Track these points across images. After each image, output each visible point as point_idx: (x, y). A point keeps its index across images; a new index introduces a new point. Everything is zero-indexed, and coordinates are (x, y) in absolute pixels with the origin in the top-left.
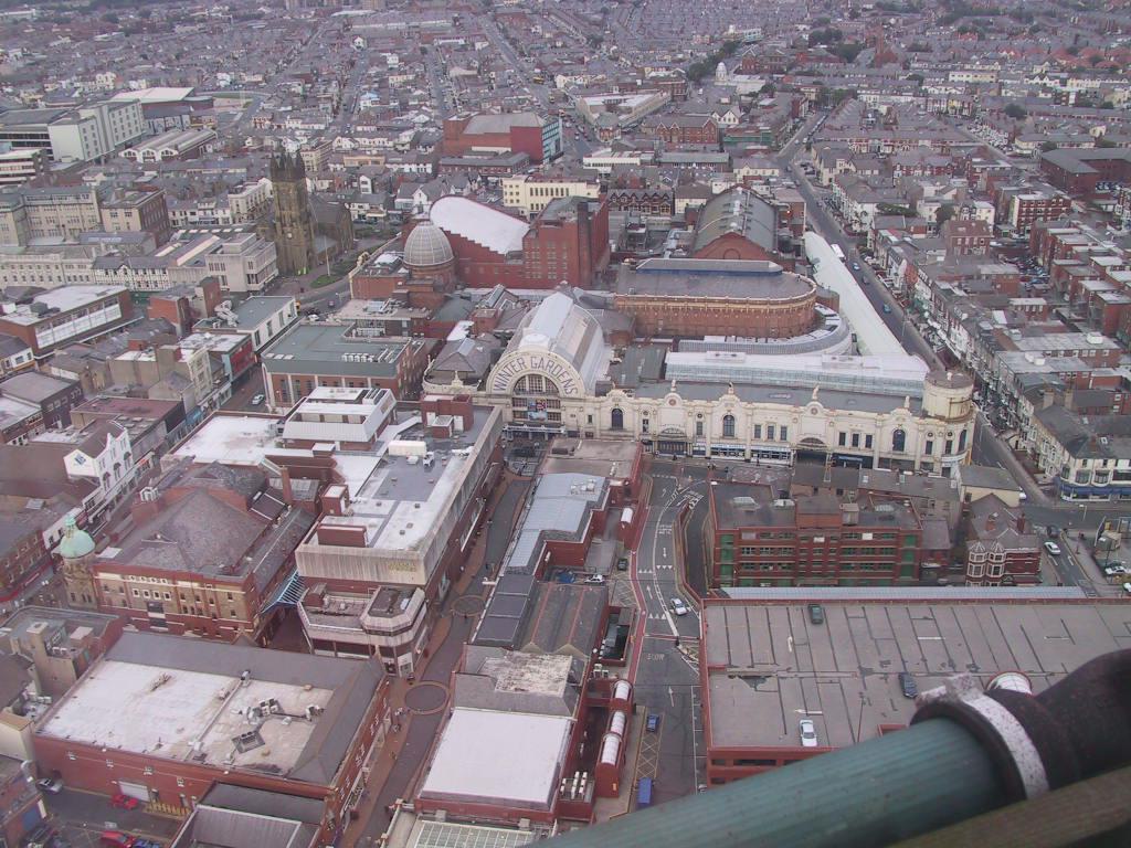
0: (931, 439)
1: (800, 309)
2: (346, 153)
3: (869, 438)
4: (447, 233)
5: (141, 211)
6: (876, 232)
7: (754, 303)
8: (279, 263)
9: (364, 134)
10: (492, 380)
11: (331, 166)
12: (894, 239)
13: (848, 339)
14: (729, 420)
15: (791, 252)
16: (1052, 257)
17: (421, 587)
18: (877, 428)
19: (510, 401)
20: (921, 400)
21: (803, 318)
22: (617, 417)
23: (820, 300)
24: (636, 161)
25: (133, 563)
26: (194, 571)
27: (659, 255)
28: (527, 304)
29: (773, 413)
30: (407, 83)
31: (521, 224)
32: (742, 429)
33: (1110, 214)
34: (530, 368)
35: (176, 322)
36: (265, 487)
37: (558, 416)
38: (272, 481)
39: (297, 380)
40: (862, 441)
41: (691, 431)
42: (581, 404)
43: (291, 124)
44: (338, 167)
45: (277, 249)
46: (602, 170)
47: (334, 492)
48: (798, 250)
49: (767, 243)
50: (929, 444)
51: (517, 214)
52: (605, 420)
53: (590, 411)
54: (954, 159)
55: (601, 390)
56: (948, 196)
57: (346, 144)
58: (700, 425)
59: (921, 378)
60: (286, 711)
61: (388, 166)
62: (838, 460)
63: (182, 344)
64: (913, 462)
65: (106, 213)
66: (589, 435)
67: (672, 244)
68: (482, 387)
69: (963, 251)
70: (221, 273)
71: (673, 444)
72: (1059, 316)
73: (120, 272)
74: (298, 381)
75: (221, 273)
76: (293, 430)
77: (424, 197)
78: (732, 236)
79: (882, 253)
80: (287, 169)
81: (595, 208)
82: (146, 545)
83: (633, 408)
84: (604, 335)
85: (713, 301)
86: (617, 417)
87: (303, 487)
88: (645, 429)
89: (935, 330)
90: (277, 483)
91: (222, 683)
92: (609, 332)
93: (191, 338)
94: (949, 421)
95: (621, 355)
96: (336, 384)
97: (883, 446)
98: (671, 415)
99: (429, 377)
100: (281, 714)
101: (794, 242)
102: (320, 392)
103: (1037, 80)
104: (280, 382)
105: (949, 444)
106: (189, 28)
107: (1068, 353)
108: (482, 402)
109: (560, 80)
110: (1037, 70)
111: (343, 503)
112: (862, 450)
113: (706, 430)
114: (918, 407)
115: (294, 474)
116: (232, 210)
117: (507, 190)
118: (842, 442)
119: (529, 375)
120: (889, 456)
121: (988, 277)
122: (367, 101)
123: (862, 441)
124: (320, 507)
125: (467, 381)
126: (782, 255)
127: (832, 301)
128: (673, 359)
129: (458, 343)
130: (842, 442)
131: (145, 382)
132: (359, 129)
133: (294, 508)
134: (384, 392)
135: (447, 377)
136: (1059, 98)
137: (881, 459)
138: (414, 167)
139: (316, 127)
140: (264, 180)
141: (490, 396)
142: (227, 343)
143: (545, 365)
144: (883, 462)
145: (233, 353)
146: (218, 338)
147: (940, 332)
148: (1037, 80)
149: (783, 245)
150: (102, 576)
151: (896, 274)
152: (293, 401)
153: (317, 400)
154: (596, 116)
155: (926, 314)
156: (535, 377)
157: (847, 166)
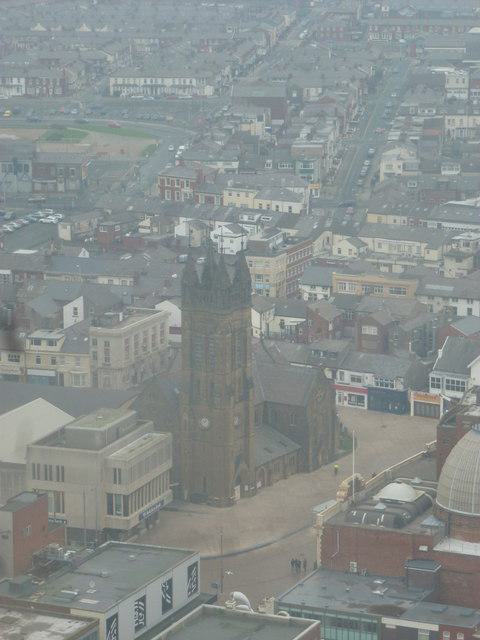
2: (341, 265)
8: (174, 474)
9: (383, 232)
11: (306, 290)
43: (234, 198)
44: (320, 292)
57: (343, 247)
61: (425, 301)
70: (54, 485)
80: (216, 288)
116: (95, 357)
122: (394, 161)
132: (372, 218)
139: (284, 207)
140: (166, 306)
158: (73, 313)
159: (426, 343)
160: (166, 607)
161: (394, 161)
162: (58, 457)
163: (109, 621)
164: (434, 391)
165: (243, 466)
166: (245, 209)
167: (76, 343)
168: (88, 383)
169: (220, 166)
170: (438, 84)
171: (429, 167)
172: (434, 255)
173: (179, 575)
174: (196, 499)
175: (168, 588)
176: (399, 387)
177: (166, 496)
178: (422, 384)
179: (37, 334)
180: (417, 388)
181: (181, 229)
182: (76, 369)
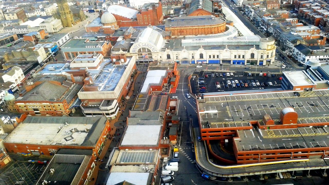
0: (262, 55)
1: (221, 26)
4: (114, 14)
5: (17, 14)
14: (201, 56)
16: (299, 8)
17: (116, 99)
19: (137, 54)
20: (259, 46)
23: (227, 24)
25: (27, 100)
26: (47, 100)
27: (178, 16)
28: (139, 31)
29: (215, 52)
31: (136, 11)
34: (142, 46)
35: (33, 41)
37: (151, 57)
42: (157, 54)
45: (62, 22)
47: (86, 79)
48: (220, 12)
49: (211, 11)
50: (262, 57)
51: (133, 8)
53: (160, 55)
55: (163, 50)
58: (193, 57)
59: (259, 40)
60: (79, 130)
63: (35, 46)
64: (257, 61)
67: (182, 13)
68: (129, 51)
69: (271, 8)
70: (44, 28)
72: (303, 23)
74: (73, 53)
75: (44, 28)
79: (246, 10)
82: (30, 96)
83: (173, 54)
84: (163, 37)
87: (79, 78)
88: (177, 58)
89: (263, 28)
91: (59, 126)
92: (164, 36)
94: (267, 50)
95: (169, 41)
97: (248, 57)
98: (184, 54)
100: (77, 131)
101: (219, 10)
102: (79, 55)
107: (304, 31)
113: (195, 57)
114: (258, 47)
119: (142, 48)
120: (249, 60)
124: (83, 83)
125: (124, 50)
126: (215, 13)
128: (183, 41)
131: (25, 56)
134: (99, 55)
137: (247, 61)
142: (49, 46)
143: (146, 45)
144: (248, 62)
145: (51, 48)
147: (264, 29)
149: (216, 11)
150: (18, 104)
151: (251, 15)
152: (72, 58)
153: (79, 58)
155: (260, 25)
156: (144, 49)
158: (41, 7)
159: (95, 4)
162: (44, 25)
163: (58, 43)
164: (98, 9)
165: (72, 22)
167: (43, 10)
168: (46, 15)
174: (66, 27)
176: (92, 9)
178: (96, 8)
179: (36, 10)
180: (95, 9)
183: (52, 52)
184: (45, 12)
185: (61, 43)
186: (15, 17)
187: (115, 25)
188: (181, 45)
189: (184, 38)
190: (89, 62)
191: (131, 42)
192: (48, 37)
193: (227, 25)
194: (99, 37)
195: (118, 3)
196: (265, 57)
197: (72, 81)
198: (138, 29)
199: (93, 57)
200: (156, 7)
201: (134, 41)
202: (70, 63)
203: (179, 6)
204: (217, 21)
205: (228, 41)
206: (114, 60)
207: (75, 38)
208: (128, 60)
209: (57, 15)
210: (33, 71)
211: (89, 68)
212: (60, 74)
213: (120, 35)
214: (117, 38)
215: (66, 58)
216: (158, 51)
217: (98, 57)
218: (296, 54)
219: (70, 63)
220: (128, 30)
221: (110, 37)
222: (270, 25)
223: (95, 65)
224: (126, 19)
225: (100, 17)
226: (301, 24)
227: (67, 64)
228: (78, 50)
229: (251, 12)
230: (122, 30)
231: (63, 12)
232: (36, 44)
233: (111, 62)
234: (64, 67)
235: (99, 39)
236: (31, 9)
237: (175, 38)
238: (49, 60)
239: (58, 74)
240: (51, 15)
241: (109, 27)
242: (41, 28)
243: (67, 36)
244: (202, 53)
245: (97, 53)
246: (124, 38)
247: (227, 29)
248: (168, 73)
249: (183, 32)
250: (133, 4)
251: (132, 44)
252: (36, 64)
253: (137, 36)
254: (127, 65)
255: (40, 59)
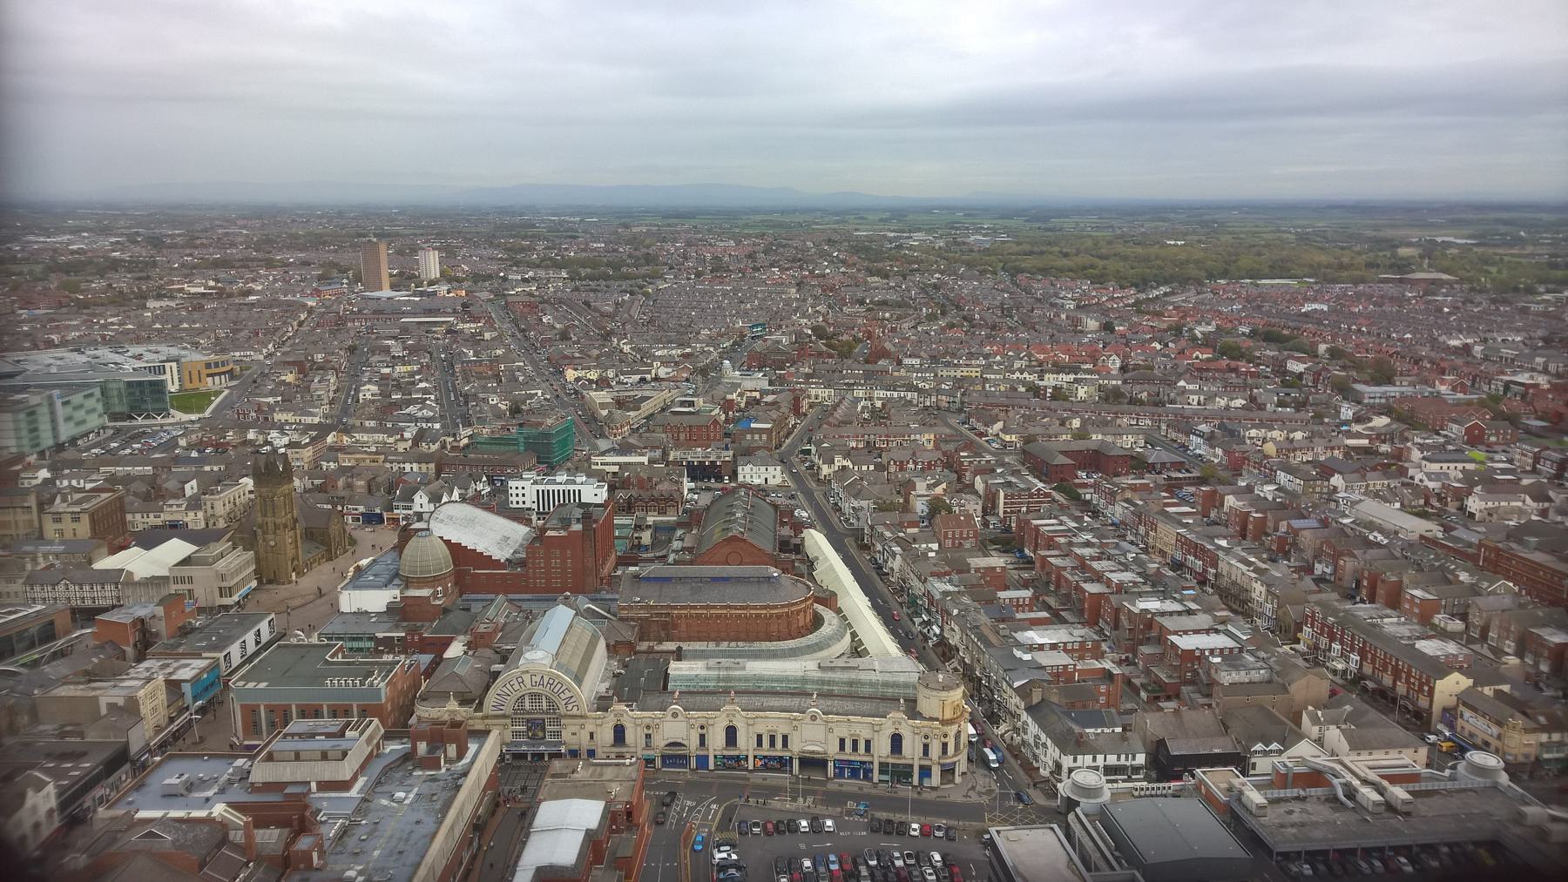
1: (798, 612)
2: (342, 449)
3: (868, 743)
4: (448, 542)
5: (92, 516)
6: (872, 528)
7: (755, 608)
10: (491, 699)
12: (888, 534)
13: (848, 637)
14: (731, 733)
15: (792, 554)
18: (876, 733)
21: (802, 620)
22: (619, 732)
23: (819, 600)
24: (645, 460)
28: (530, 617)
29: (773, 722)
30: (412, 374)
32: (745, 744)
33: (1089, 502)
36: (224, 841)
38: (232, 833)
39: (271, 710)
40: (862, 746)
41: (694, 742)
43: (279, 417)
44: (332, 465)
45: (258, 560)
46: (607, 468)
47: (304, 843)
48: (798, 549)
49: (768, 546)
50: (926, 747)
52: (608, 735)
53: (590, 727)
54: (944, 454)
55: (603, 703)
56: (939, 490)
59: (914, 678)
62: (841, 766)
65: (47, 519)
66: (591, 753)
67: (676, 545)
68: (480, 707)
71: (675, 756)
72: (1048, 608)
73: (61, 587)
76: (262, 773)
77: (425, 500)
78: (734, 538)
79: (879, 547)
81: (601, 515)
85: (714, 607)
86: (619, 732)
87: (270, 837)
90: (237, 837)
93: (146, 664)
94: (944, 722)
95: (625, 666)
96: (317, 714)
97: (882, 748)
98: (674, 727)
99: (423, 699)
102: (297, 725)
103: (1018, 374)
104: (251, 712)
105: (945, 745)
106: (165, 303)
107: (1054, 647)
108: (479, 726)
109: (571, 374)
110: (1017, 365)
111: (315, 855)
112: (861, 755)
113: (709, 741)
115: (260, 823)
117: (513, 491)
118: (842, 747)
121: (977, 570)
123: (862, 746)
127: (829, 599)
128: (677, 669)
129: (455, 660)
130: (842, 747)
133: (258, 865)
135: (443, 696)
136: (1035, 391)
138: (415, 466)
139: (309, 420)
140: (244, 480)
141: (486, 717)
144: (884, 768)
145: (195, 680)
146: (176, 665)
148: (1018, 374)
149: (785, 546)
153: (293, 735)
154: (604, 413)
157: (845, 463)
158: (191, 488)
159: (390, 490)
160: (257, 643)
161: (369, 391)
162: (187, 571)
166: (287, 422)
167: (195, 504)
168: (203, 525)
169: (271, 400)
170: (387, 350)
171: (385, 394)
172: (391, 440)
173: (264, 626)
174: (270, 582)
175: (258, 633)
176: (378, 511)
177: (254, 584)
178: (390, 509)
181: (251, 435)
182: (195, 520)
183: (195, 699)
184: (200, 514)
185: (236, 660)
186: (84, 528)
187: (445, 589)
188: (665, 687)
189: (679, 655)
190: (324, 756)
191: (496, 667)
192: (194, 630)
193: (820, 608)
194: (380, 635)
195: (471, 493)
196: (935, 751)
197: (243, 855)
198: (525, 606)
199: (343, 735)
200: (596, 521)
201: (504, 660)
202: (252, 758)
203: (671, 518)
204: (790, 592)
205: (820, 674)
206: (422, 747)
207: (294, 641)
208: (473, 747)
209: (244, 530)
210: (99, 792)
211: (325, 786)
212: (202, 814)
213: (458, 632)
214: (446, 643)
215: (240, 734)
216: (584, 709)
217: (361, 734)
218: (1032, 741)
219: (252, 758)
220: (491, 612)
221: (422, 639)
222: (950, 614)
223: (345, 771)
224: (488, 561)
225: (400, 548)
226: (1045, 614)
227: (240, 762)
228: (294, 695)
229: (894, 555)
230: (468, 610)
231: (269, 520)
232: (140, 658)
233: (408, 757)
234: (226, 777)
235: (379, 641)
236: (154, 494)
237: (650, 651)
238: (173, 743)
239: (196, 814)
240: (221, 524)
241: (425, 592)
242: (173, 588)
243: (264, 626)
244: (735, 723)
245: (365, 712)
246: (469, 645)
247: (817, 622)
248: (610, 816)
249: (675, 626)
250: (521, 499)
251: (496, 675)
252: (120, 758)
253: (515, 640)
254: (465, 774)
255: (139, 737)
